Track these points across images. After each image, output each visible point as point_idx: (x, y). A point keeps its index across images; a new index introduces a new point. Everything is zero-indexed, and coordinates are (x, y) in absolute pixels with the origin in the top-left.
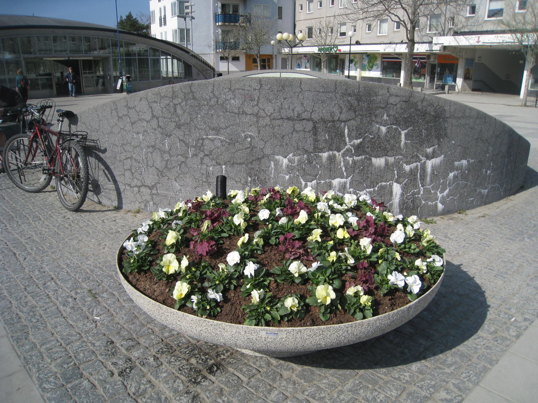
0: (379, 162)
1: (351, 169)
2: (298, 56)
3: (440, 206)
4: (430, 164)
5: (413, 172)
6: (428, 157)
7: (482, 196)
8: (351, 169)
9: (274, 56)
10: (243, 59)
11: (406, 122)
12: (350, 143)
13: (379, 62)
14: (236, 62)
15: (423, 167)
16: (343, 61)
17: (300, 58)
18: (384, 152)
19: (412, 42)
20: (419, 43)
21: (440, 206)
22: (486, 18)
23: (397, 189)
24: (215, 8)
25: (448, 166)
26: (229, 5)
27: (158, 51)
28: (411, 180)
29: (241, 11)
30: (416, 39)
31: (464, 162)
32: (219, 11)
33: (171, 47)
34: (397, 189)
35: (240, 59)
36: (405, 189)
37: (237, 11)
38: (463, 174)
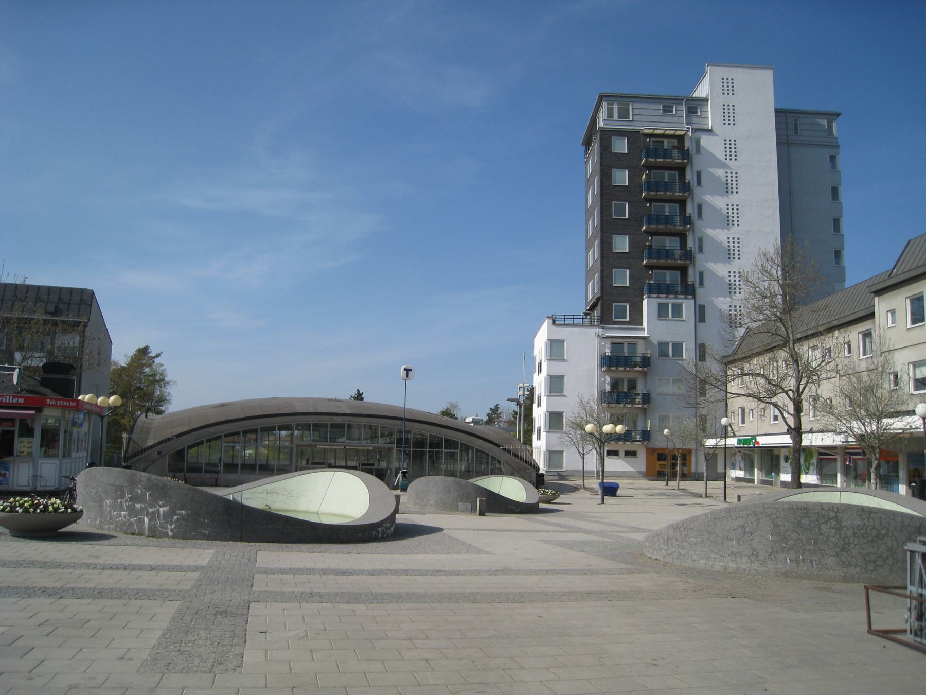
0: (138, 506)
1: (128, 508)
2: (733, 451)
3: (170, 533)
4: (161, 510)
5: (153, 513)
6: (161, 506)
7: (204, 534)
8: (128, 508)
9: (693, 452)
10: (642, 455)
11: (149, 489)
12: (128, 496)
13: (814, 461)
14: (631, 459)
15: (158, 511)
16: (778, 457)
17: (735, 454)
18: (140, 502)
19: (796, 432)
20: (811, 431)
21: (170, 533)
22: (912, 391)
23: (146, 520)
24: (601, 384)
25: (172, 512)
26: (623, 380)
27: (183, 450)
28: (152, 517)
29: (640, 388)
30: (805, 426)
31: (184, 512)
32: (608, 388)
33: (475, 439)
34: (146, 520)
35: (638, 454)
36: (150, 520)
37: (635, 387)
38: (183, 518)
